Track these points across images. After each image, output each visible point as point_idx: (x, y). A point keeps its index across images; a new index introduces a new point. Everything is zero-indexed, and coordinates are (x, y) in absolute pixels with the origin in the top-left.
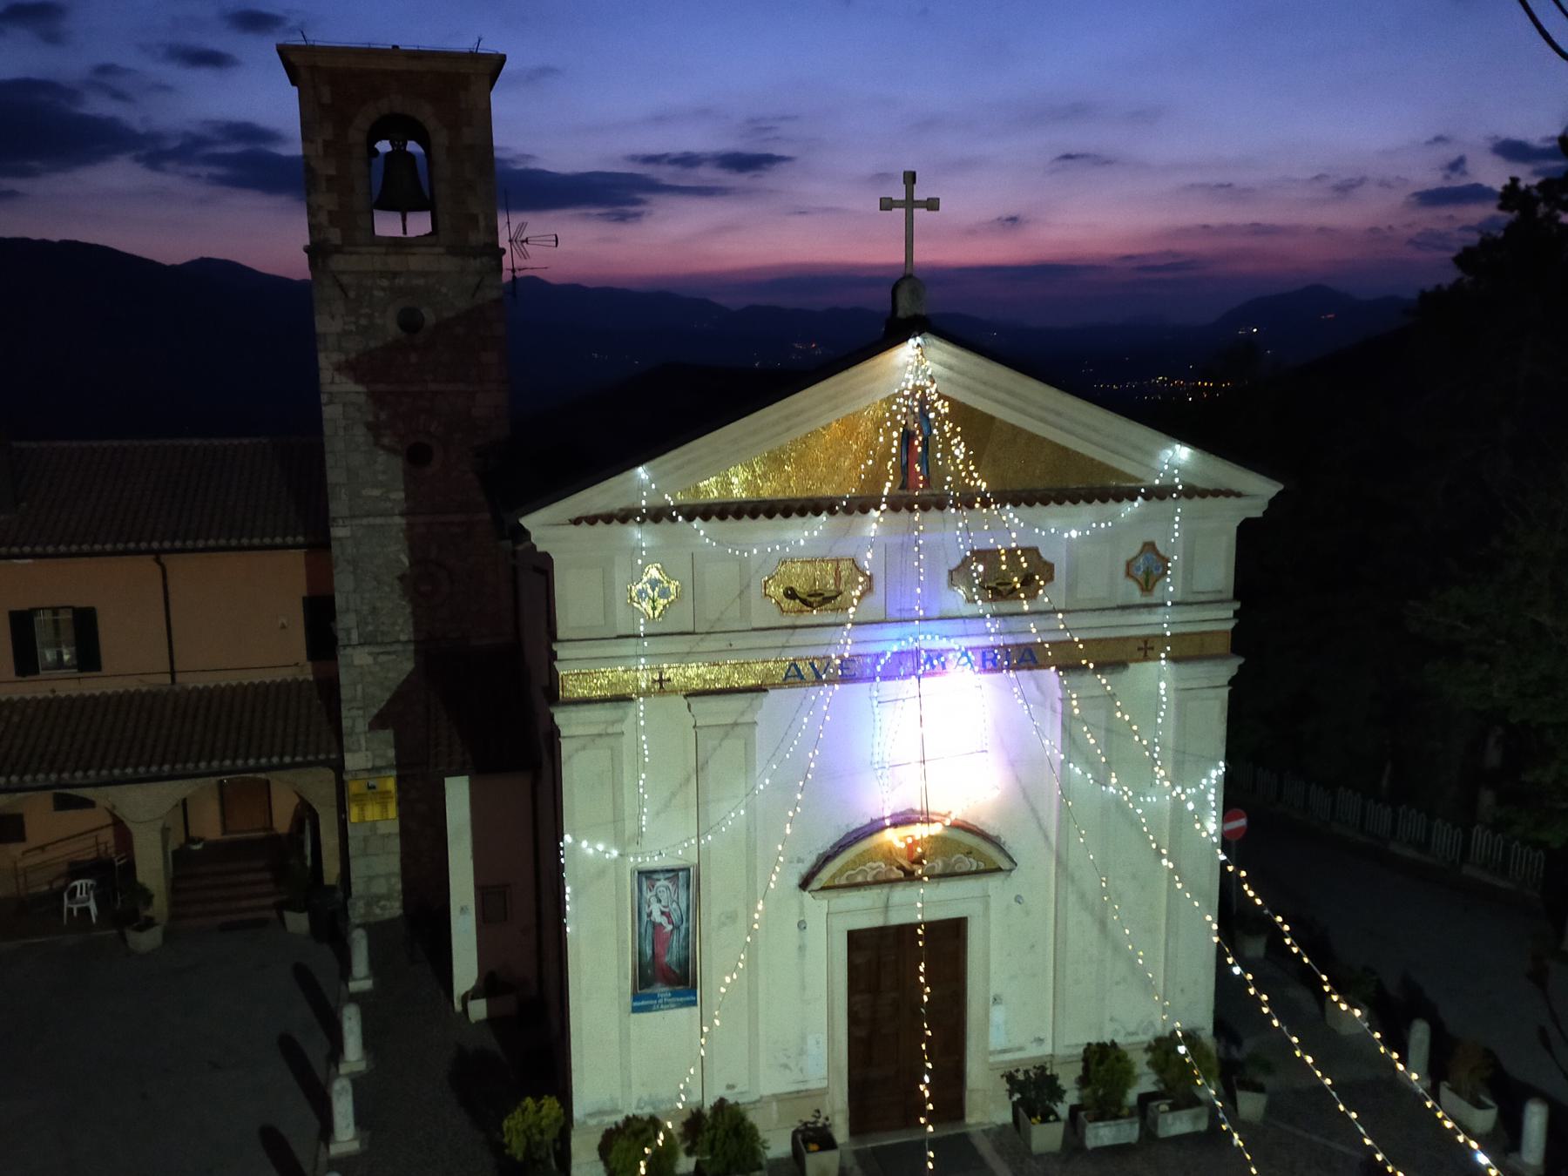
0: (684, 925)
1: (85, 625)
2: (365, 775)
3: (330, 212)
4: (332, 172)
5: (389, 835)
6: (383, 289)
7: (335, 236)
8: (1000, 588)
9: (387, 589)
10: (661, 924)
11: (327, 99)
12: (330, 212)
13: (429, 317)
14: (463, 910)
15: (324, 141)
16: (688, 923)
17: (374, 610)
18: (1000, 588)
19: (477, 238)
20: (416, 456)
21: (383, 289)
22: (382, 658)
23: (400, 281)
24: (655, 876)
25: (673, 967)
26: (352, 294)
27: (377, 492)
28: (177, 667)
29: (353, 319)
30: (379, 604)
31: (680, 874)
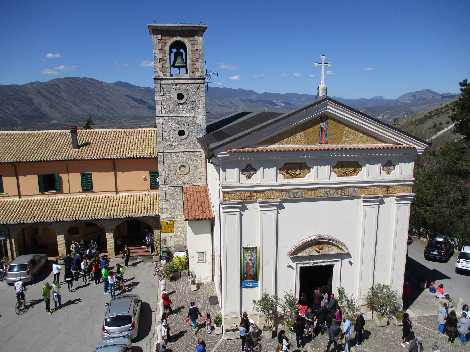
0: (256, 264)
3: (160, 68)
6: (173, 88)
8: (347, 172)
9: (172, 170)
10: (249, 263)
16: (255, 262)
18: (347, 172)
19: (198, 75)
21: (173, 88)
22: (171, 188)
24: (247, 250)
25: (252, 275)
26: (165, 90)
27: (170, 143)
31: (255, 249)
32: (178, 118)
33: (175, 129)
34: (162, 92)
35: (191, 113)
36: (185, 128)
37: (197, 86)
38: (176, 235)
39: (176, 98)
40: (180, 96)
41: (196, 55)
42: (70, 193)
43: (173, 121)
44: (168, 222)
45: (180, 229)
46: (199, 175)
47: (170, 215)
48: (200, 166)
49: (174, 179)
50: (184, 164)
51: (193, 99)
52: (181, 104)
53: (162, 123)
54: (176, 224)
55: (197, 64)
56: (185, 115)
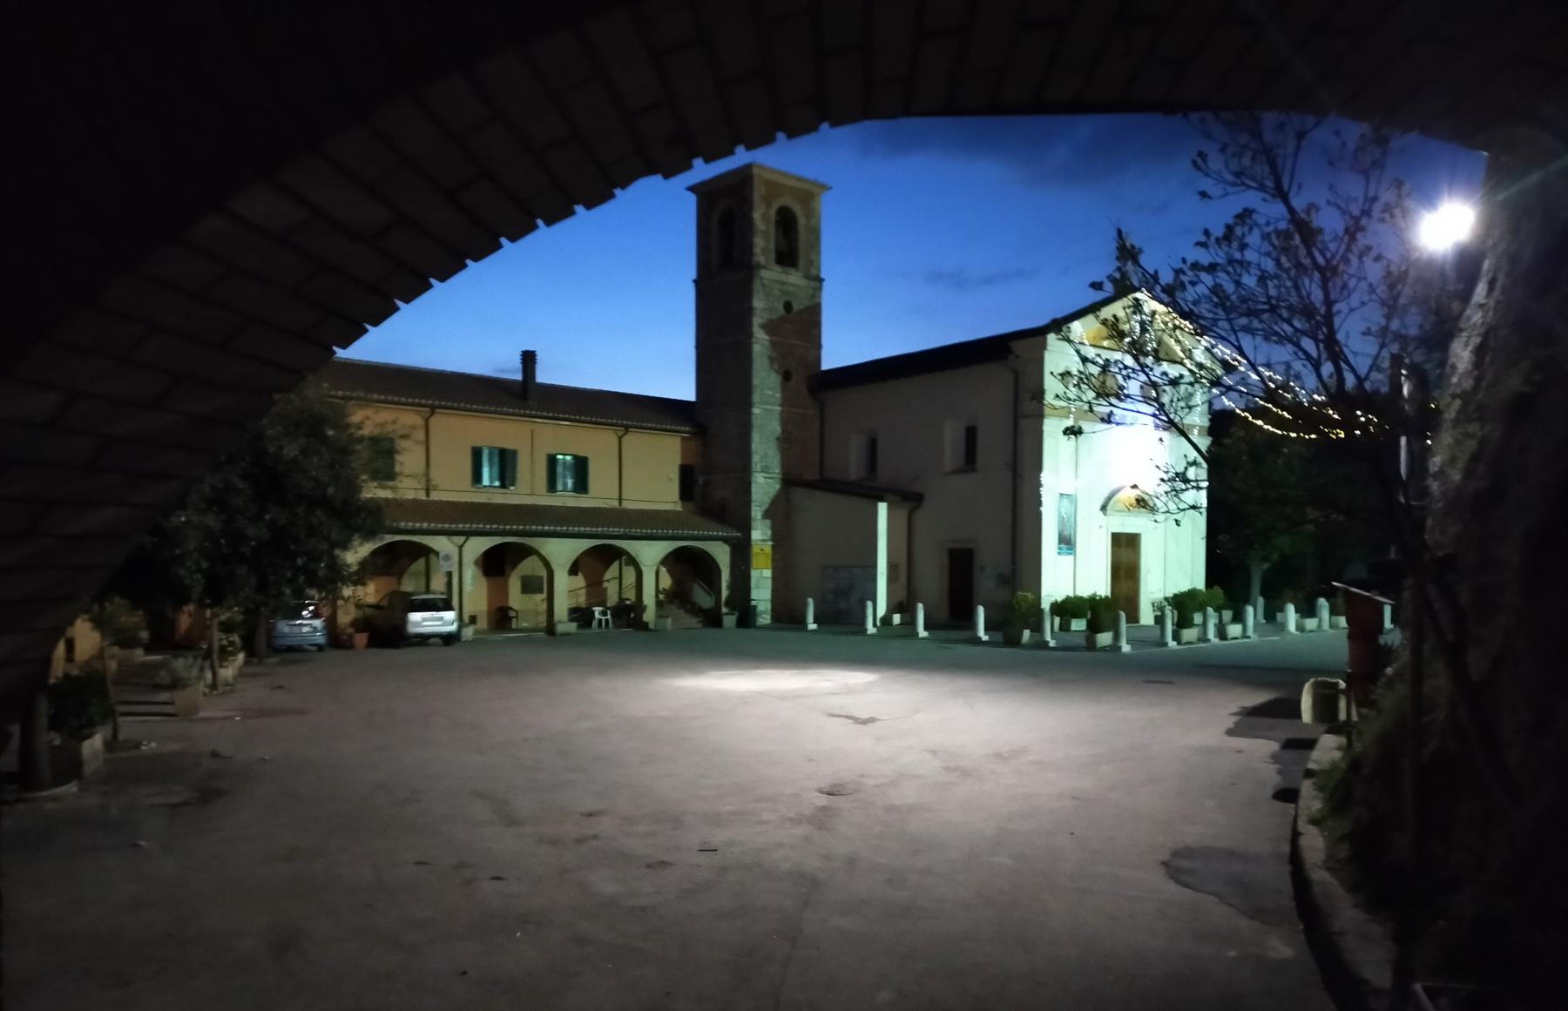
1: (581, 467)
2: (760, 543)
5: (767, 578)
13: (796, 307)
14: (882, 574)
20: (786, 376)
23: (785, 287)
27: (770, 392)
28: (624, 497)
37: (811, 292)
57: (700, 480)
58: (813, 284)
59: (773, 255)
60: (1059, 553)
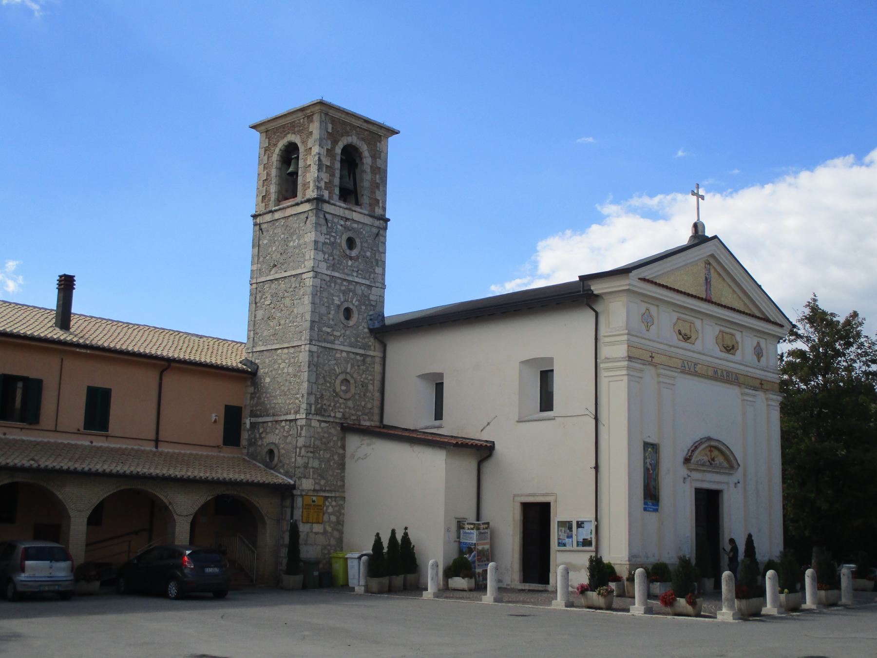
3: (325, 182)
4: (328, 164)
6: (341, 225)
7: (326, 195)
9: (328, 385)
11: (330, 130)
12: (325, 182)
15: (327, 149)
17: (322, 396)
21: (341, 225)
22: (323, 425)
26: (330, 225)
27: (329, 330)
28: (161, 438)
29: (328, 237)
30: (324, 393)
32: (345, 283)
33: (339, 303)
34: (325, 228)
35: (365, 278)
36: (354, 305)
37: (375, 230)
38: (325, 532)
39: (344, 245)
40: (351, 243)
41: (377, 176)
42: (56, 431)
43: (336, 288)
44: (314, 498)
45: (333, 518)
46: (369, 406)
47: (319, 484)
48: (370, 387)
49: (329, 406)
50: (349, 378)
51: (368, 254)
52: (351, 258)
53: (321, 287)
54: (328, 507)
55: (377, 192)
56: (357, 280)
57: (247, 422)
58: (377, 223)
59: (337, 191)
60: (645, 509)
